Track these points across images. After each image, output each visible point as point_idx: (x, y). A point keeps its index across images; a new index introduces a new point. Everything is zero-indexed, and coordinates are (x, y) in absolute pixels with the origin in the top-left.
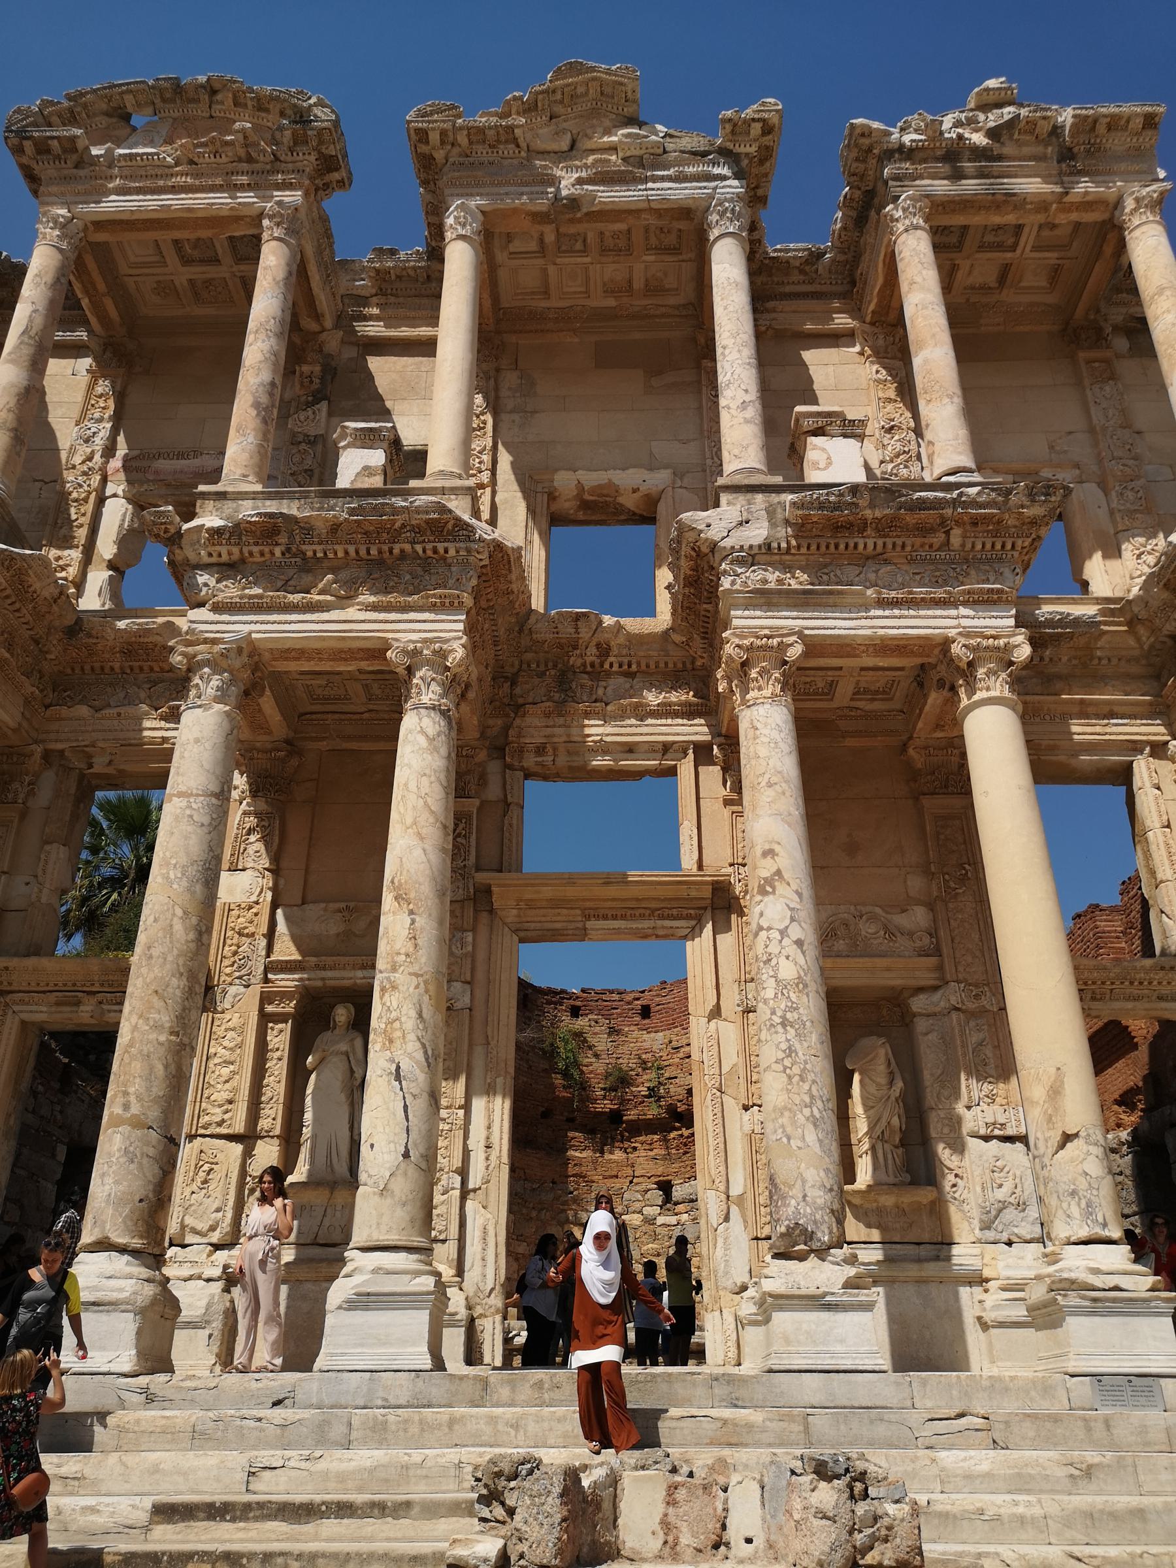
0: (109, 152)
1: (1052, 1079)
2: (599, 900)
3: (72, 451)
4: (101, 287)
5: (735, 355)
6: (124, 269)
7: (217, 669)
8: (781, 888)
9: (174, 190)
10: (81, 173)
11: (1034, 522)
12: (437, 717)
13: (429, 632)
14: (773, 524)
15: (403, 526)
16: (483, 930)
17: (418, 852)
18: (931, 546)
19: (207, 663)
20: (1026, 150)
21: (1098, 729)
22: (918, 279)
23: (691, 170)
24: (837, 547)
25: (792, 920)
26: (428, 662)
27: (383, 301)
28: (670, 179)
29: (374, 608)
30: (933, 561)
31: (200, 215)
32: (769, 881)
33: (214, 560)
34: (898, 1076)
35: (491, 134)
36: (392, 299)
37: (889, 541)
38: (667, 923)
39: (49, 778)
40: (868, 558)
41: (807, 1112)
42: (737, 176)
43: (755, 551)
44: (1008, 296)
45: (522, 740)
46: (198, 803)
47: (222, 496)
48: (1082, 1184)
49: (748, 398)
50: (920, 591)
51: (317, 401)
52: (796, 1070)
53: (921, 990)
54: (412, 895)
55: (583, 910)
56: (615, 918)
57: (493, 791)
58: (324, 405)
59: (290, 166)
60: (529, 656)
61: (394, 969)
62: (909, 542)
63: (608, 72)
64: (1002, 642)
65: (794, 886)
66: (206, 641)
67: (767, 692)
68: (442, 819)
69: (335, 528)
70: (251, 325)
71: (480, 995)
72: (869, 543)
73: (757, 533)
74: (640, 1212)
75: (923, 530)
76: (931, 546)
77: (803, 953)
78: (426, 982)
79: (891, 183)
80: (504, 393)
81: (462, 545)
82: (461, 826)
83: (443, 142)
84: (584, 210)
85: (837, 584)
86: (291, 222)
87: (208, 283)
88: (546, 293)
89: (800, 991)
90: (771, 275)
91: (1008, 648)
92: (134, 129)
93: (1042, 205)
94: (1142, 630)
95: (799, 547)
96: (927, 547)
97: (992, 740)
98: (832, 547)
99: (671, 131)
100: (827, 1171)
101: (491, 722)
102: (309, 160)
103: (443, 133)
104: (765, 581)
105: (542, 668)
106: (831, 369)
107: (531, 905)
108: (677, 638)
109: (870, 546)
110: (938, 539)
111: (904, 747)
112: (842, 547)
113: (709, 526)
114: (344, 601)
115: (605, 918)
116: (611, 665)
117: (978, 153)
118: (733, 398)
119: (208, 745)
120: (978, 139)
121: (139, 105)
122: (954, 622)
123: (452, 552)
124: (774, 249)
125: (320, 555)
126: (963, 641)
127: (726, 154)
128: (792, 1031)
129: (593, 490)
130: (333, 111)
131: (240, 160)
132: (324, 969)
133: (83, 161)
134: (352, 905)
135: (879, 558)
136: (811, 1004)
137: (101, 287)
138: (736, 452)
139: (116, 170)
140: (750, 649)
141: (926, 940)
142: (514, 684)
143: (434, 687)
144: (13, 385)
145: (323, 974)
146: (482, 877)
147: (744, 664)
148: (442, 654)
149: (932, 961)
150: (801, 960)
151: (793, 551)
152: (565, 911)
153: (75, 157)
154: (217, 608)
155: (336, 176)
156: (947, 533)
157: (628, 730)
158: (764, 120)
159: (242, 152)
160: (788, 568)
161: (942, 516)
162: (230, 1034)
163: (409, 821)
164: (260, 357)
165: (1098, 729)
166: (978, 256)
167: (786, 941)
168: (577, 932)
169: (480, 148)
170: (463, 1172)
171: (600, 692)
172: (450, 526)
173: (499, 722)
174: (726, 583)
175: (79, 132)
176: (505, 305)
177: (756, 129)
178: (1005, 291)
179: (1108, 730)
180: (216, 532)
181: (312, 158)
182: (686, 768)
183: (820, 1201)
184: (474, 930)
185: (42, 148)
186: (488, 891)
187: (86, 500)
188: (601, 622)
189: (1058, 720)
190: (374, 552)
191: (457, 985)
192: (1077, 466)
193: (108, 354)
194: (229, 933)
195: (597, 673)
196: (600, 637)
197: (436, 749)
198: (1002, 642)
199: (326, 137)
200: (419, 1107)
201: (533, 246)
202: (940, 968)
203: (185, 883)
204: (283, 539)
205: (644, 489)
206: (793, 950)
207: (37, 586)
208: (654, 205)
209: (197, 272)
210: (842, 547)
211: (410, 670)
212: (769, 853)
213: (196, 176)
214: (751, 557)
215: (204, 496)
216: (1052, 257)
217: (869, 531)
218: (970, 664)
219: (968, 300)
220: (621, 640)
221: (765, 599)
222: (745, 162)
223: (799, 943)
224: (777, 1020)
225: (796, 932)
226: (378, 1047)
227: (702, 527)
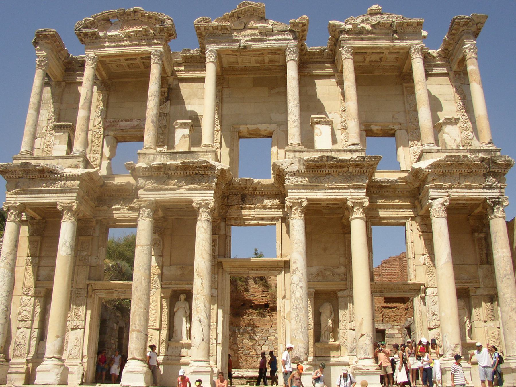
0: (105, 34)
3: (94, 121)
5: (292, 103)
7: (147, 207)
8: (297, 272)
9: (125, 46)
10: (98, 40)
11: (372, 165)
12: (206, 222)
13: (203, 197)
14: (300, 165)
16: (220, 274)
17: (203, 262)
19: (144, 207)
20: (383, 31)
21: (397, 213)
22: (348, 77)
23: (280, 37)
25: (300, 281)
26: (204, 206)
27: (186, 64)
29: (189, 189)
32: (295, 270)
34: (333, 314)
35: (219, 28)
36: (189, 64)
38: (272, 272)
39: (98, 227)
41: (300, 330)
42: (295, 39)
44: (383, 63)
46: (145, 248)
47: (145, 154)
48: (364, 346)
49: (296, 118)
50: (340, 185)
51: (167, 101)
52: (298, 320)
53: (341, 290)
54: (202, 274)
55: (248, 268)
56: (257, 270)
57: (222, 232)
58: (169, 102)
59: (159, 37)
61: (198, 294)
63: (255, 5)
64: (361, 201)
65: (301, 272)
66: (143, 201)
67: (297, 215)
68: (209, 252)
69: (177, 167)
70: (149, 94)
71: (220, 292)
72: (327, 171)
73: (296, 167)
74: (274, 336)
79: (342, 42)
80: (224, 96)
81: (212, 171)
83: (205, 29)
85: (318, 183)
86: (160, 56)
87: (132, 64)
91: (363, 202)
92: (112, 24)
94: (409, 184)
99: (275, 22)
100: (304, 344)
101: (221, 211)
103: (205, 27)
104: (297, 182)
106: (328, 87)
107: (233, 267)
108: (277, 186)
109: (327, 172)
111: (342, 219)
112: (319, 172)
114: (180, 187)
115: (254, 270)
117: (369, 32)
118: (291, 118)
119: (146, 231)
120: (368, 27)
122: (349, 194)
123: (210, 173)
124: (310, 49)
126: (351, 200)
127: (290, 31)
128: (298, 310)
129: (252, 131)
130: (172, 21)
131: (144, 35)
132: (177, 284)
133: (98, 37)
134: (184, 266)
135: (330, 174)
138: (291, 137)
139: (107, 39)
140: (292, 202)
141: (343, 276)
142: (228, 199)
143: (206, 214)
144: (84, 117)
145: (177, 286)
146: (220, 259)
147: (291, 207)
148: (208, 204)
149: (344, 282)
150: (301, 292)
154: (146, 190)
157: (262, 213)
158: (302, 23)
162: (154, 302)
163: (200, 254)
164: (152, 105)
165: (397, 213)
167: (298, 287)
169: (216, 31)
170: (216, 339)
171: (253, 201)
173: (224, 211)
174: (286, 182)
175: (96, 30)
176: (224, 66)
177: (300, 25)
179: (400, 213)
180: (145, 168)
181: (165, 35)
182: (279, 223)
183: (302, 351)
184: (218, 274)
185: (86, 34)
186: (221, 262)
187: (100, 137)
188: (253, 181)
190: (188, 173)
191: (214, 290)
192: (400, 124)
193: (103, 86)
194: (152, 276)
195: (253, 196)
196: (253, 185)
197: (207, 232)
198: (361, 201)
200: (206, 329)
202: (346, 284)
203: (144, 270)
204: (163, 170)
205: (268, 130)
206: (299, 289)
209: (129, 62)
210: (319, 172)
211: (199, 208)
212: (295, 263)
213: (131, 41)
215: (139, 154)
218: (353, 207)
220: (259, 186)
221: (297, 187)
222: (297, 34)
223: (301, 287)
224: (295, 307)
225: (301, 284)
226: (195, 313)
227: (280, 165)
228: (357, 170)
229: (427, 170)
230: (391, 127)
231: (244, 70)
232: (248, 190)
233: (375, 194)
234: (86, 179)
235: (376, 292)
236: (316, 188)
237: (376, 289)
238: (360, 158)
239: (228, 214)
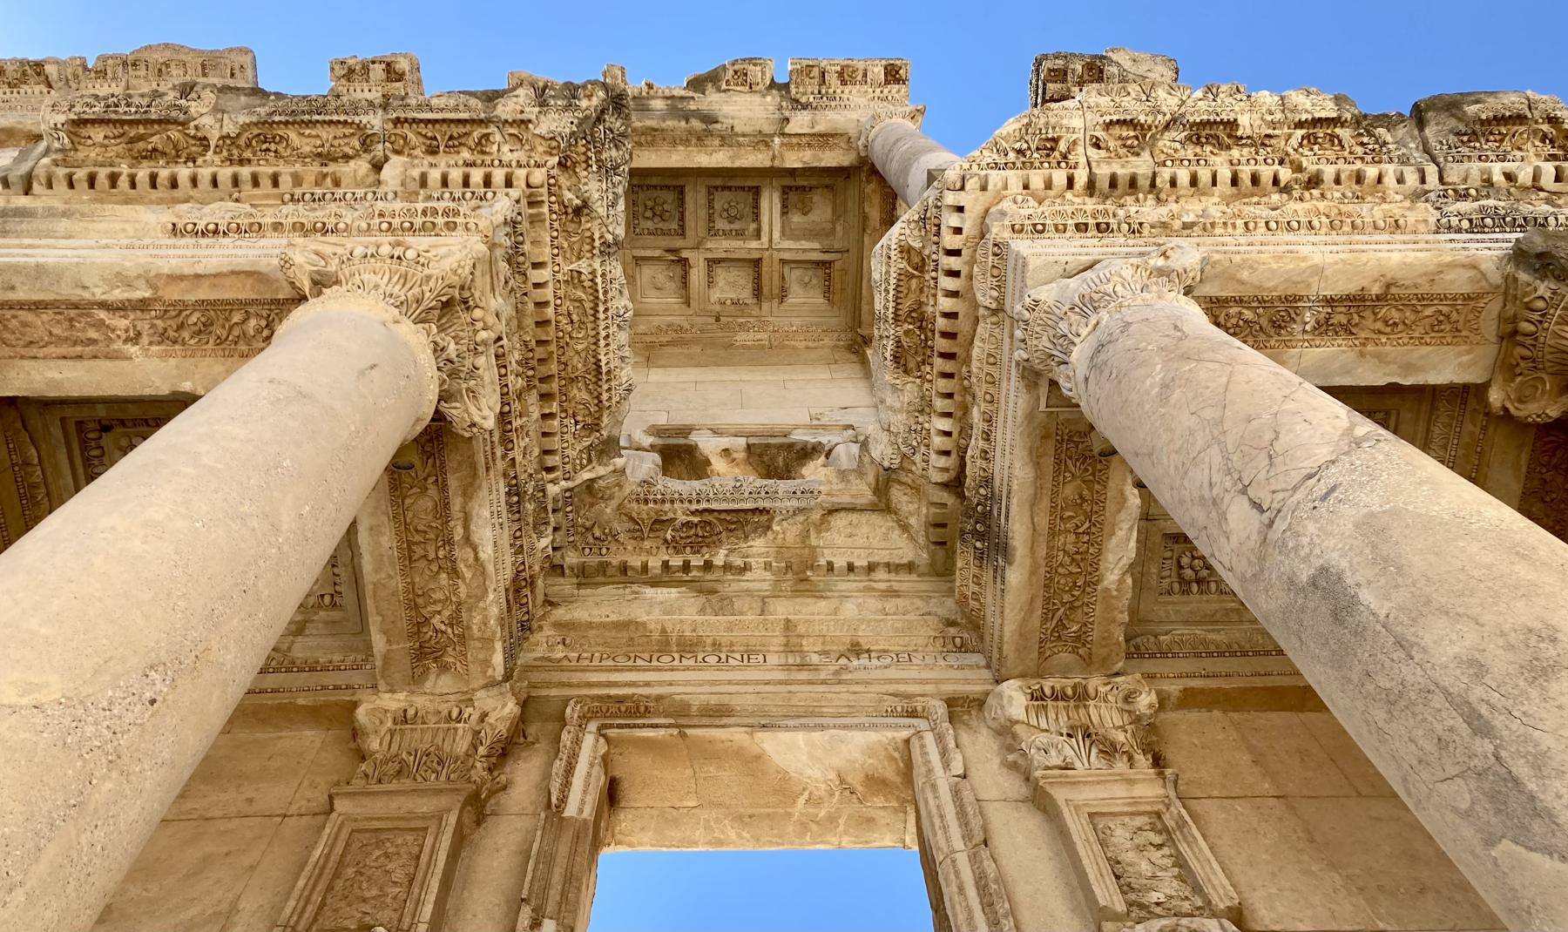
37: (245, 172)
98: (123, 182)
156: (377, 167)
178: (765, 306)
233: (655, 583)
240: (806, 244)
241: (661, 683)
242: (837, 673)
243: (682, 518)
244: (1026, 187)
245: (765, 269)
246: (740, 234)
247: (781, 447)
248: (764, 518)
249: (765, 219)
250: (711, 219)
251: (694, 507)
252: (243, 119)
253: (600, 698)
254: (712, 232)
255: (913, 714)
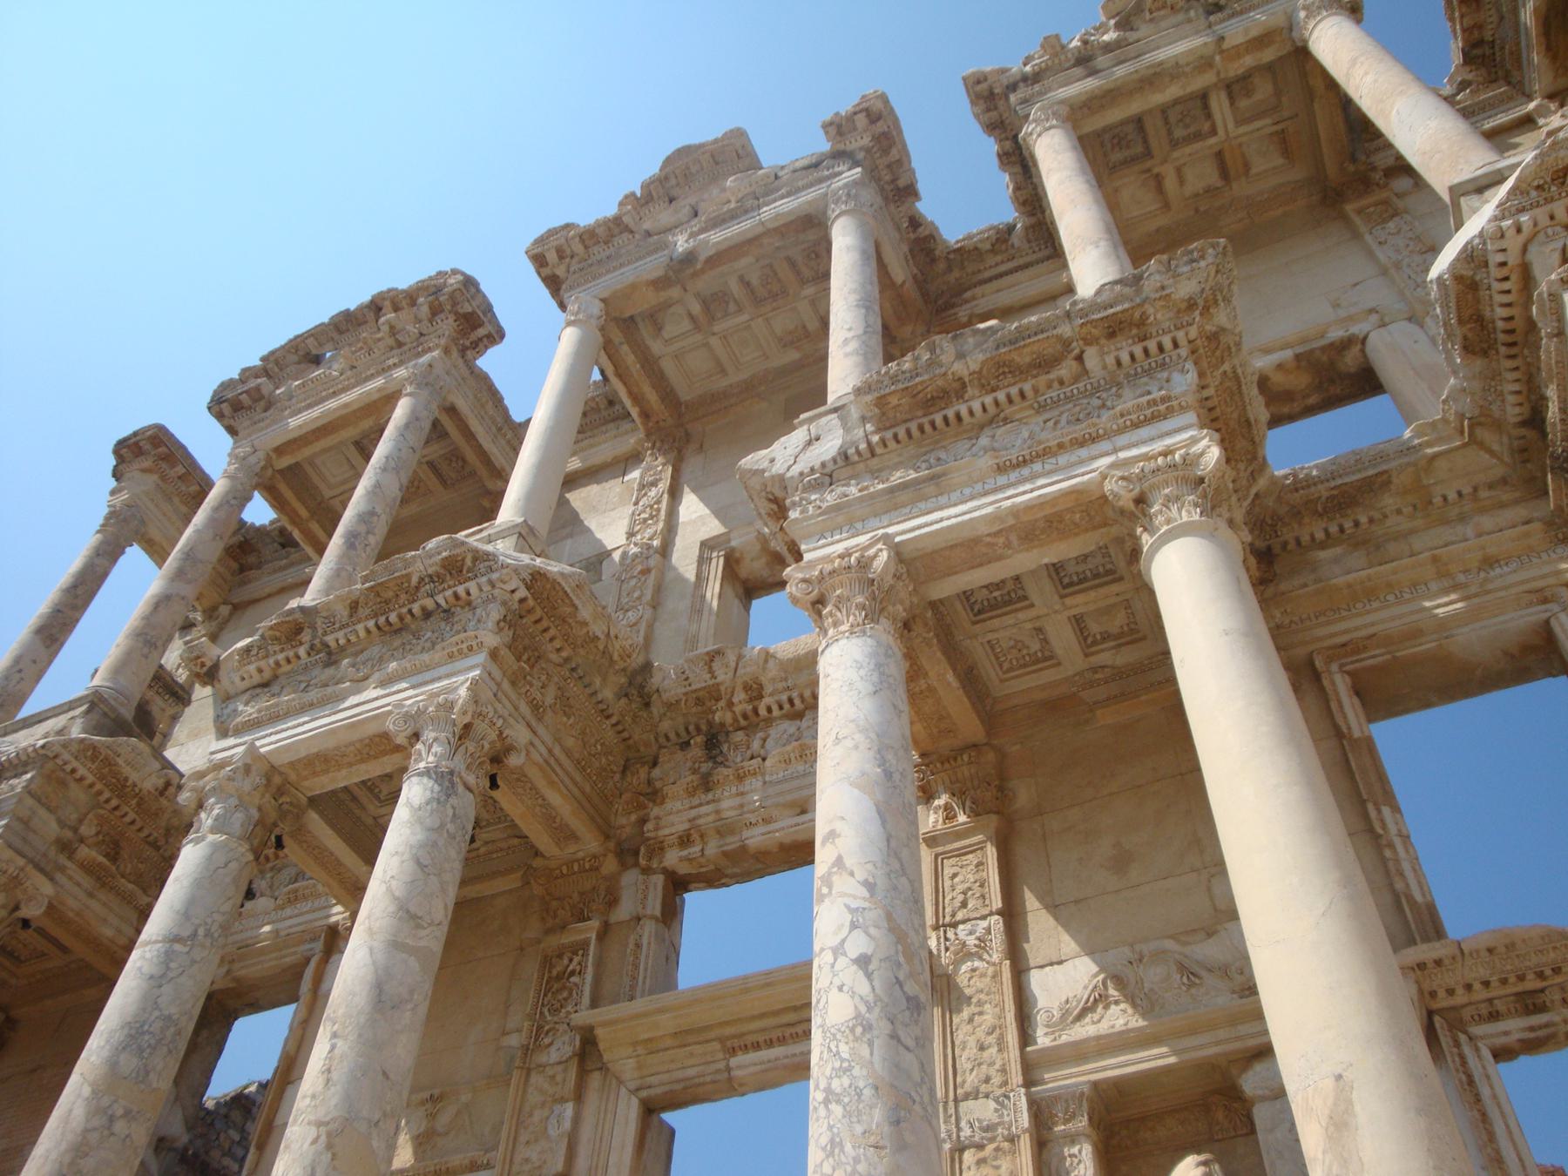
1: (1330, 1102)
2: (740, 1020)
4: (304, 513)
6: (327, 493)
15: (421, 579)
18: (1061, 383)
24: (933, 424)
25: (854, 926)
28: (783, 197)
30: (1068, 399)
31: (355, 407)
33: (247, 684)
37: (1001, 396)
40: (982, 427)
43: (831, 467)
44: (1241, 188)
45: (661, 833)
55: (722, 1040)
56: (770, 1044)
60: (665, 726)
62: (1027, 387)
65: (860, 875)
75: (1044, 364)
76: (1061, 383)
77: (869, 976)
78: (329, 1135)
81: (484, 579)
82: (576, 959)
83: (561, 257)
84: (702, 257)
88: (723, 372)
89: (856, 1039)
90: (963, 268)
93: (1204, 63)
95: (883, 442)
96: (1056, 384)
97: (1193, 591)
98: (927, 428)
102: (447, 325)
105: (685, 737)
110: (1066, 369)
113: (772, 461)
115: (757, 1046)
116: (769, 710)
121: (321, 345)
123: (474, 591)
125: (342, 642)
128: (837, 1109)
135: (996, 418)
136: (877, 1059)
137: (304, 513)
150: (864, 988)
151: (879, 450)
152: (698, 1049)
153: (262, 403)
155: (481, 332)
156: (1080, 358)
159: (391, 341)
160: (876, 474)
161: (1059, 338)
166: (1176, 154)
167: (842, 962)
168: (718, 1077)
169: (596, 249)
171: (756, 745)
172: (469, 562)
173: (633, 817)
177: (861, 120)
178: (1235, 185)
181: (451, 320)
184: (579, 1097)
189: (1407, 596)
190: (393, 617)
195: (753, 722)
196: (746, 672)
199: (458, 294)
201: (686, 325)
204: (306, 636)
207: (134, 777)
208: (770, 226)
214: (827, 476)
216: (1265, 124)
217: (970, 391)
219: (1197, 211)
220: (773, 670)
223: (863, 962)
227: (765, 464)
228: (1125, 349)
229: (1507, 223)
230: (1336, 334)
231: (749, 389)
232: (730, 704)
233: (1323, 546)
234: (82, 771)
235: (1494, 1016)
236: (930, 489)
237: (1480, 994)
238: (1118, 288)
239: (649, 826)
240: (1258, 124)
241: (1365, 626)
242: (1481, 585)
243: (1325, 494)
244: (1552, 218)
245: (1227, 155)
246: (1198, 136)
247: (1323, 349)
248: (1385, 477)
249: (1218, 117)
250: (1170, 132)
251: (1333, 484)
252: (981, 357)
253: (1330, 648)
254: (1175, 144)
255: (1545, 601)
